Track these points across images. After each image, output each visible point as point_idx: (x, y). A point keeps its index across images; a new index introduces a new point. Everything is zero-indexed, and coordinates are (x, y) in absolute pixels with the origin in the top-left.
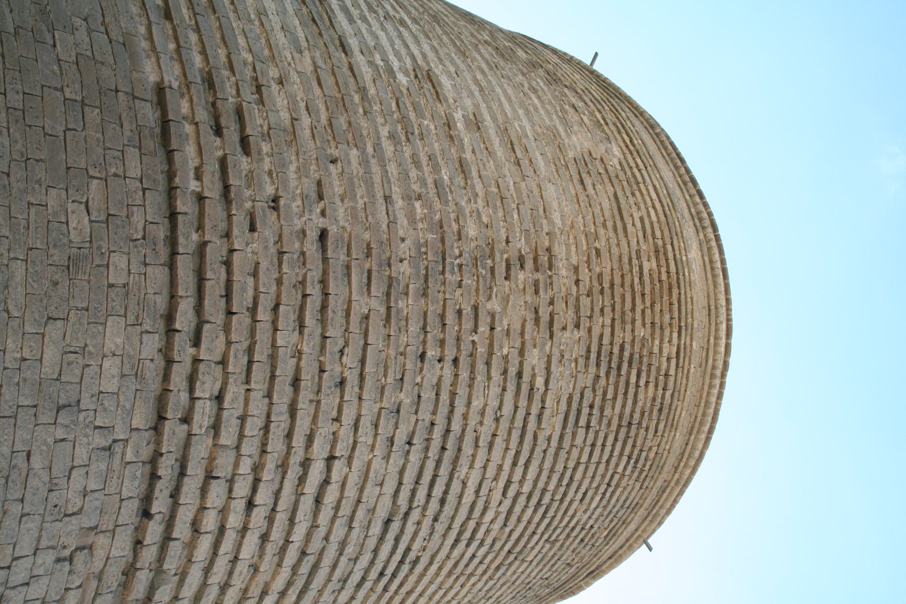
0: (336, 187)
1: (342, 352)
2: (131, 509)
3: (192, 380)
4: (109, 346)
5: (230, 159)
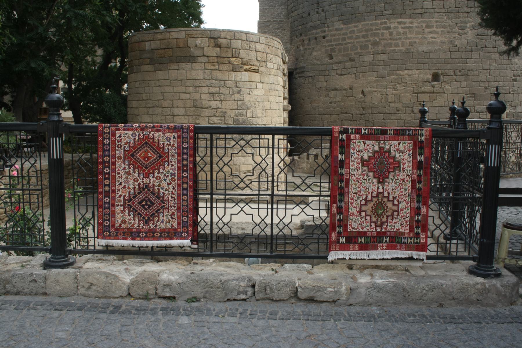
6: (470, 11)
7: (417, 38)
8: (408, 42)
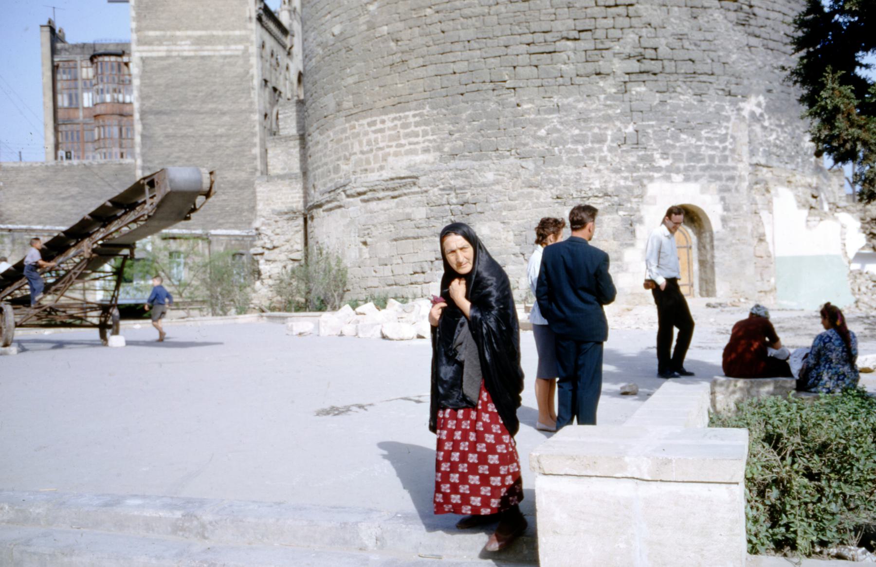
7: (391, 146)
8: (381, 156)
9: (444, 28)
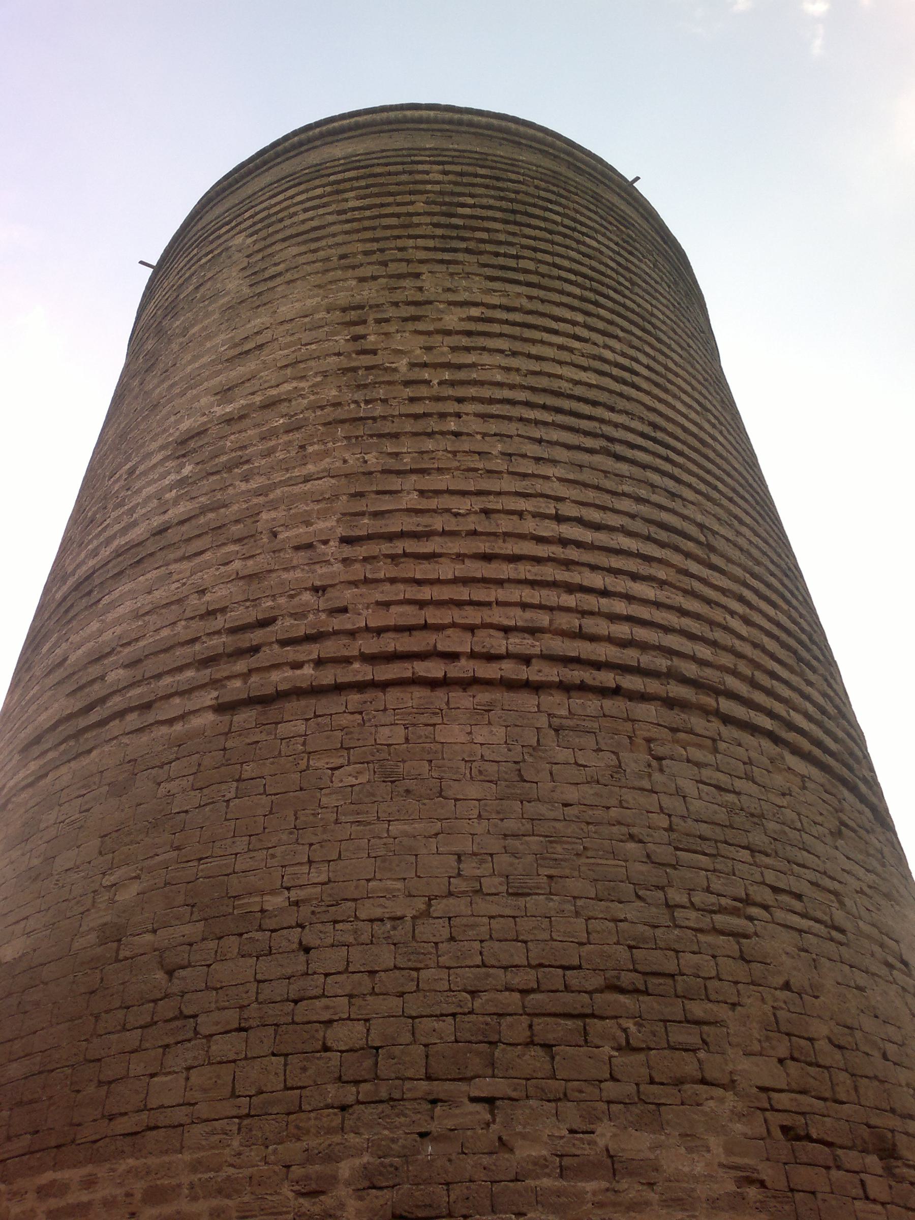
0: (300, 533)
1: (456, 515)
2: (611, 705)
3: (491, 658)
4: (463, 738)
5: (281, 637)
6: (351, 1099)
9: (310, 938)
